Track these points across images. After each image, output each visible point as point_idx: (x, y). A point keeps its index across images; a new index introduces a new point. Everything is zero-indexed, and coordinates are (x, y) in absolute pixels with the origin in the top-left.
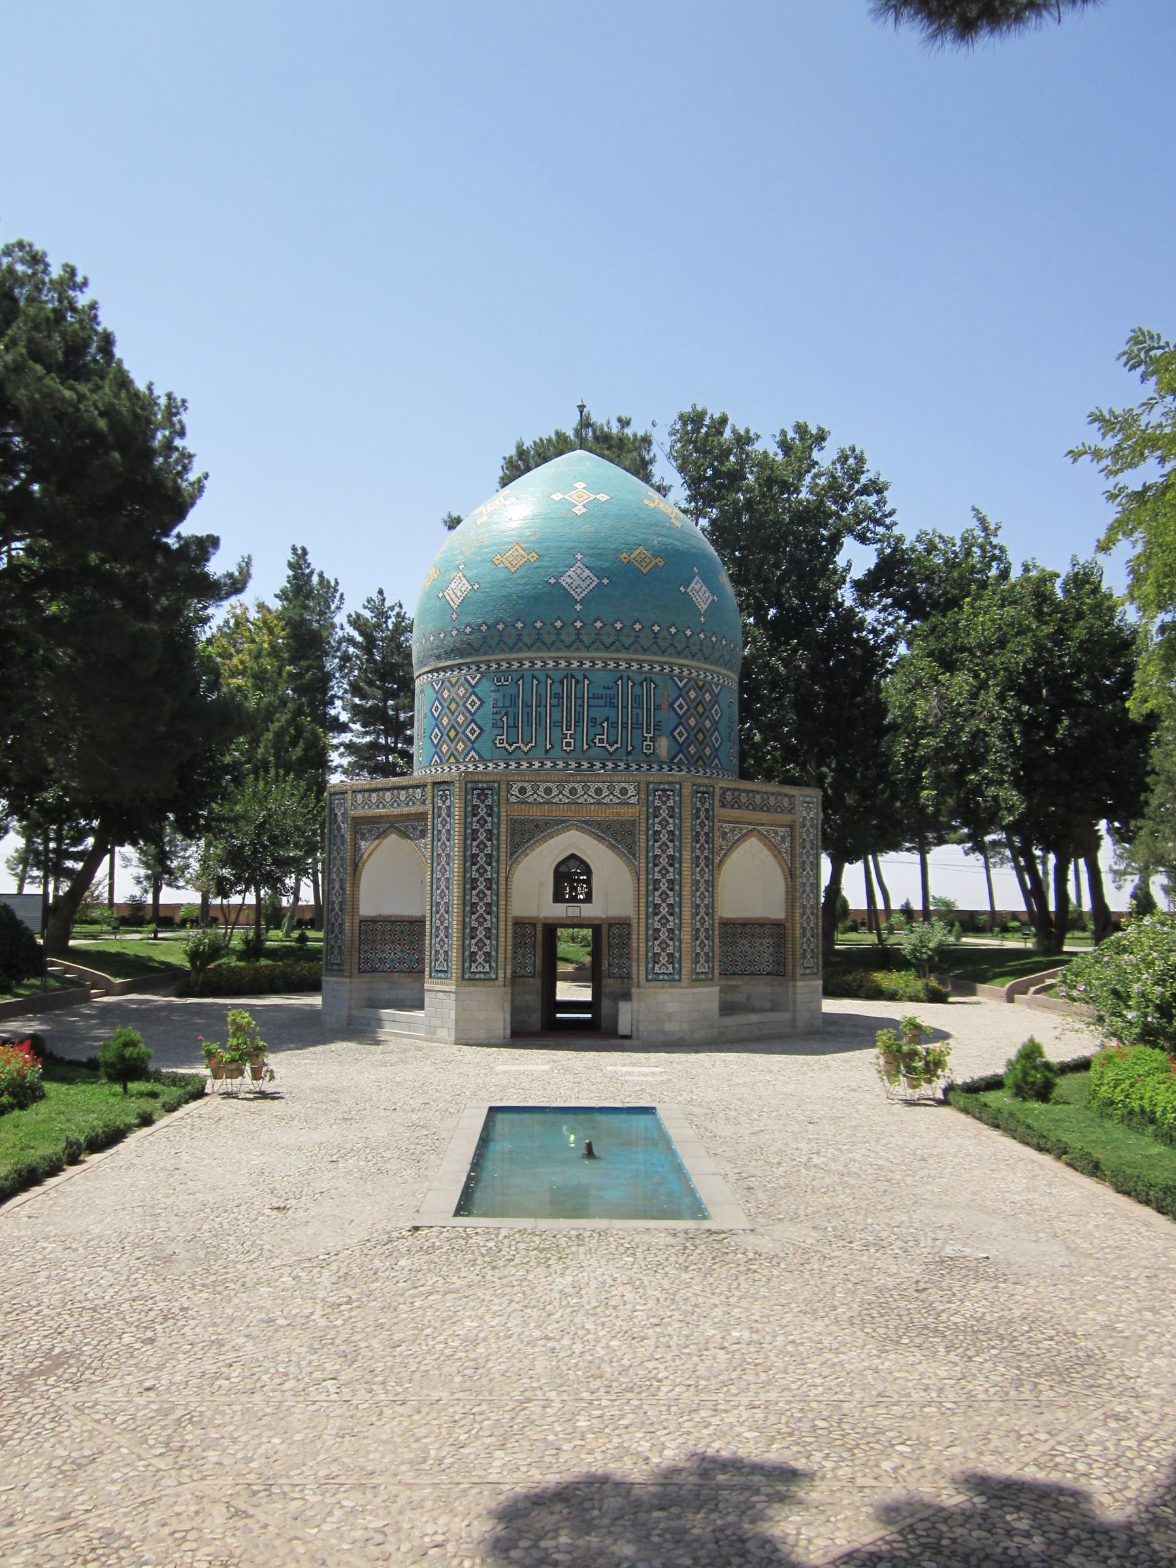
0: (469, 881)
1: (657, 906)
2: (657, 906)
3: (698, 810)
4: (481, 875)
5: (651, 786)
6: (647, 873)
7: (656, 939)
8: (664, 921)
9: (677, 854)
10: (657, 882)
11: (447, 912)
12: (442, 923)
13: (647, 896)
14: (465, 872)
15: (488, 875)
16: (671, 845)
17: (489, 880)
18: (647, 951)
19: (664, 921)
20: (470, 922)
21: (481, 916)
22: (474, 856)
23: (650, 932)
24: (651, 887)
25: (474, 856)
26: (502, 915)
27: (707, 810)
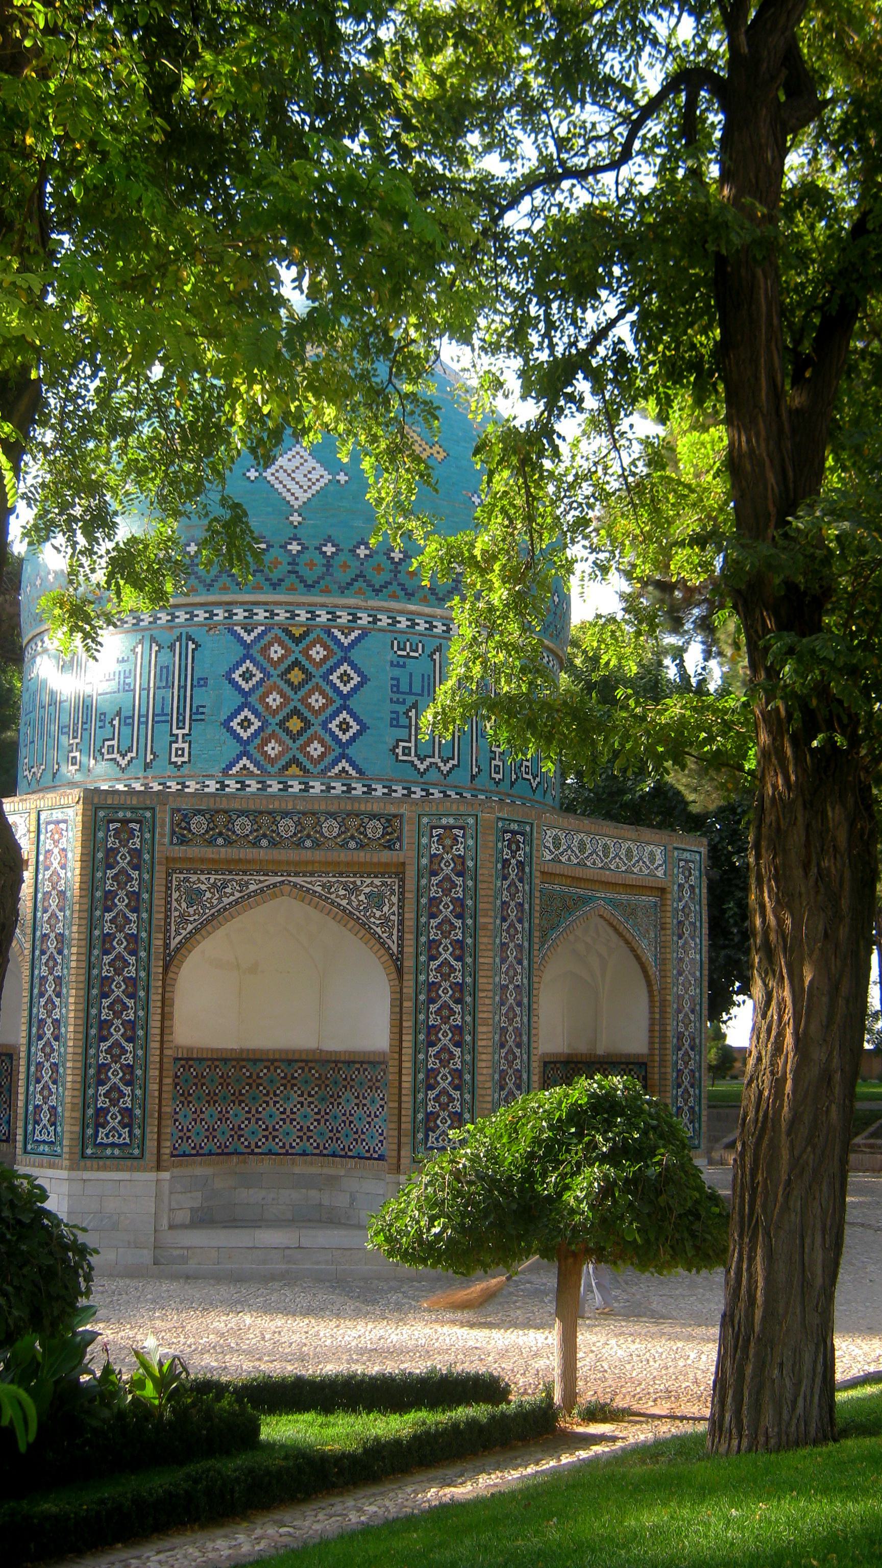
0: (97, 983)
1: (432, 1030)
2: (432, 1030)
3: (506, 863)
4: (118, 972)
5: (425, 820)
6: (417, 972)
7: (430, 1087)
8: (445, 1057)
9: (469, 941)
10: (432, 987)
11: (57, 1039)
12: (48, 1056)
13: (417, 1012)
14: (90, 967)
15: (131, 972)
16: (458, 923)
17: (132, 982)
18: (415, 1112)
19: (445, 1057)
20: (97, 1056)
21: (117, 1044)
22: (108, 938)
23: (421, 1076)
24: (422, 997)
25: (108, 938)
26: (155, 1045)
27: (520, 864)
